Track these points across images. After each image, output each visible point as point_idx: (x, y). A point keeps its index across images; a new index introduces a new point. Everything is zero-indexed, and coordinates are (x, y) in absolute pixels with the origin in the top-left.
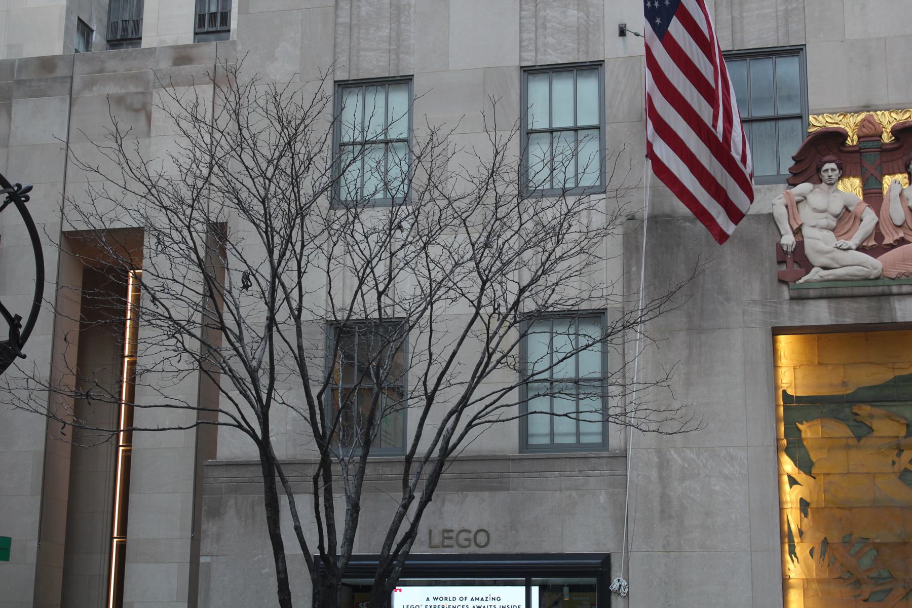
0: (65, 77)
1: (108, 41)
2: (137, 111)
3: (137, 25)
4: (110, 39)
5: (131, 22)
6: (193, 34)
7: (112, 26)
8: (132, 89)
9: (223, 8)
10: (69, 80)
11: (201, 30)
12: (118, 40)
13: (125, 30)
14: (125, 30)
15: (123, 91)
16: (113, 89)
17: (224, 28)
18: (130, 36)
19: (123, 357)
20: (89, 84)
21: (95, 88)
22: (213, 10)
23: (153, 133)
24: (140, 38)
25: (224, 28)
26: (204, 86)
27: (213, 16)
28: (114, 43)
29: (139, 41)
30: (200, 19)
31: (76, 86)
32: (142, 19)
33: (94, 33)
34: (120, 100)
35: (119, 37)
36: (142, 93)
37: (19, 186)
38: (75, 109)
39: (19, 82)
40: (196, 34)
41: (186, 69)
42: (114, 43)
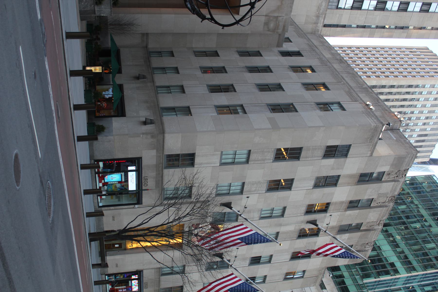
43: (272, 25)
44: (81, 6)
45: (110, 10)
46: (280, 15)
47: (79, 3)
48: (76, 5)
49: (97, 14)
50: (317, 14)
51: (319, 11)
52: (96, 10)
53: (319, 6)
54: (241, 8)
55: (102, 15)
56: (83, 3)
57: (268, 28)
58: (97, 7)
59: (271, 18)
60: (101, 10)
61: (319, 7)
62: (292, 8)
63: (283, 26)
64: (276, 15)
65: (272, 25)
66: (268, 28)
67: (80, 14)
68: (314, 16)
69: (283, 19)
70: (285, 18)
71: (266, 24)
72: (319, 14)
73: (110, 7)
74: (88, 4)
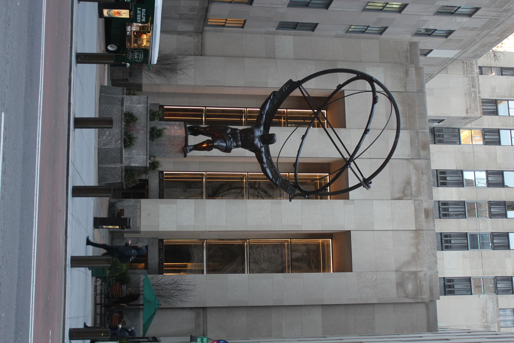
0: (419, 156)
1: (434, 128)
2: (403, 192)
3: (441, 142)
4: (435, 129)
5: (442, 139)
6: (437, 169)
7: (440, 130)
8: (414, 189)
9: (449, 183)
10: (418, 158)
11: (438, 173)
12: (434, 133)
13: (439, 136)
14: (439, 136)
15: (413, 185)
16: (414, 179)
17: (439, 184)
18: (436, 138)
19: (287, 109)
20: (416, 168)
21: (414, 170)
22: (448, 178)
23: (393, 201)
24: (435, 144)
25: (439, 184)
26: (414, 225)
27: (445, 178)
28: (433, 131)
29: (434, 143)
30: (443, 172)
31: (415, 161)
32: (444, 144)
33: (438, 124)
34: (408, 183)
35: (436, 133)
36: (412, 194)
37: (371, 183)
38: (405, 161)
39: (417, 133)
40: (437, 170)
41: (423, 216)
42: (433, 131)
43: (410, 287)
44: (101, 141)
45: (145, 157)
46: (419, 270)
47: (99, 137)
48: (95, 102)
49: (125, 163)
50: (485, 322)
51: (485, 317)
52: (124, 157)
53: (484, 309)
54: (350, 192)
55: (133, 165)
56: (104, 138)
57: (405, 292)
58: (125, 152)
59: (407, 275)
60: (131, 157)
61: (484, 311)
62: (437, 257)
63: (429, 288)
64: (413, 269)
65: (410, 287)
66: (405, 292)
67: (101, 92)
68: (481, 327)
69: (425, 275)
70: (428, 273)
71: (400, 285)
72: (487, 322)
73: (146, 153)
74: (112, 139)
